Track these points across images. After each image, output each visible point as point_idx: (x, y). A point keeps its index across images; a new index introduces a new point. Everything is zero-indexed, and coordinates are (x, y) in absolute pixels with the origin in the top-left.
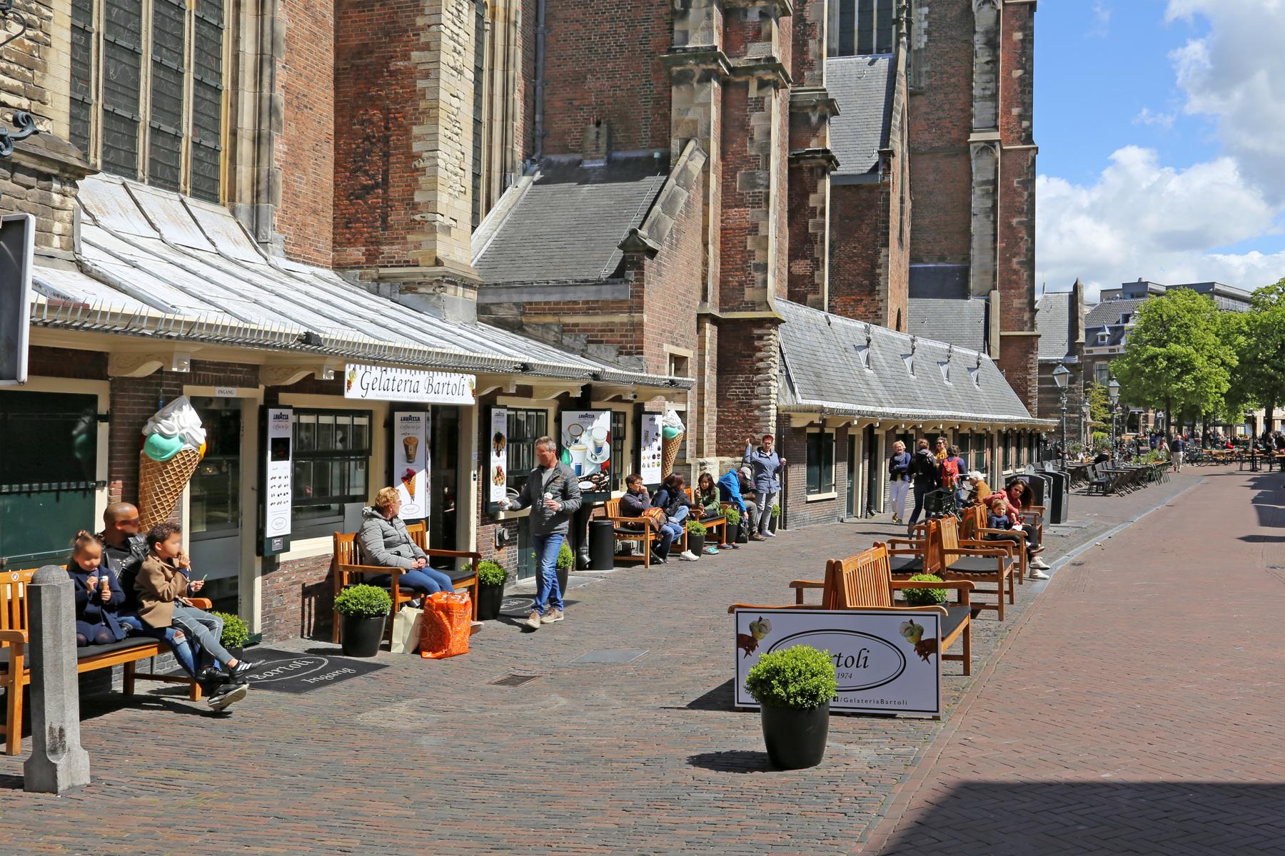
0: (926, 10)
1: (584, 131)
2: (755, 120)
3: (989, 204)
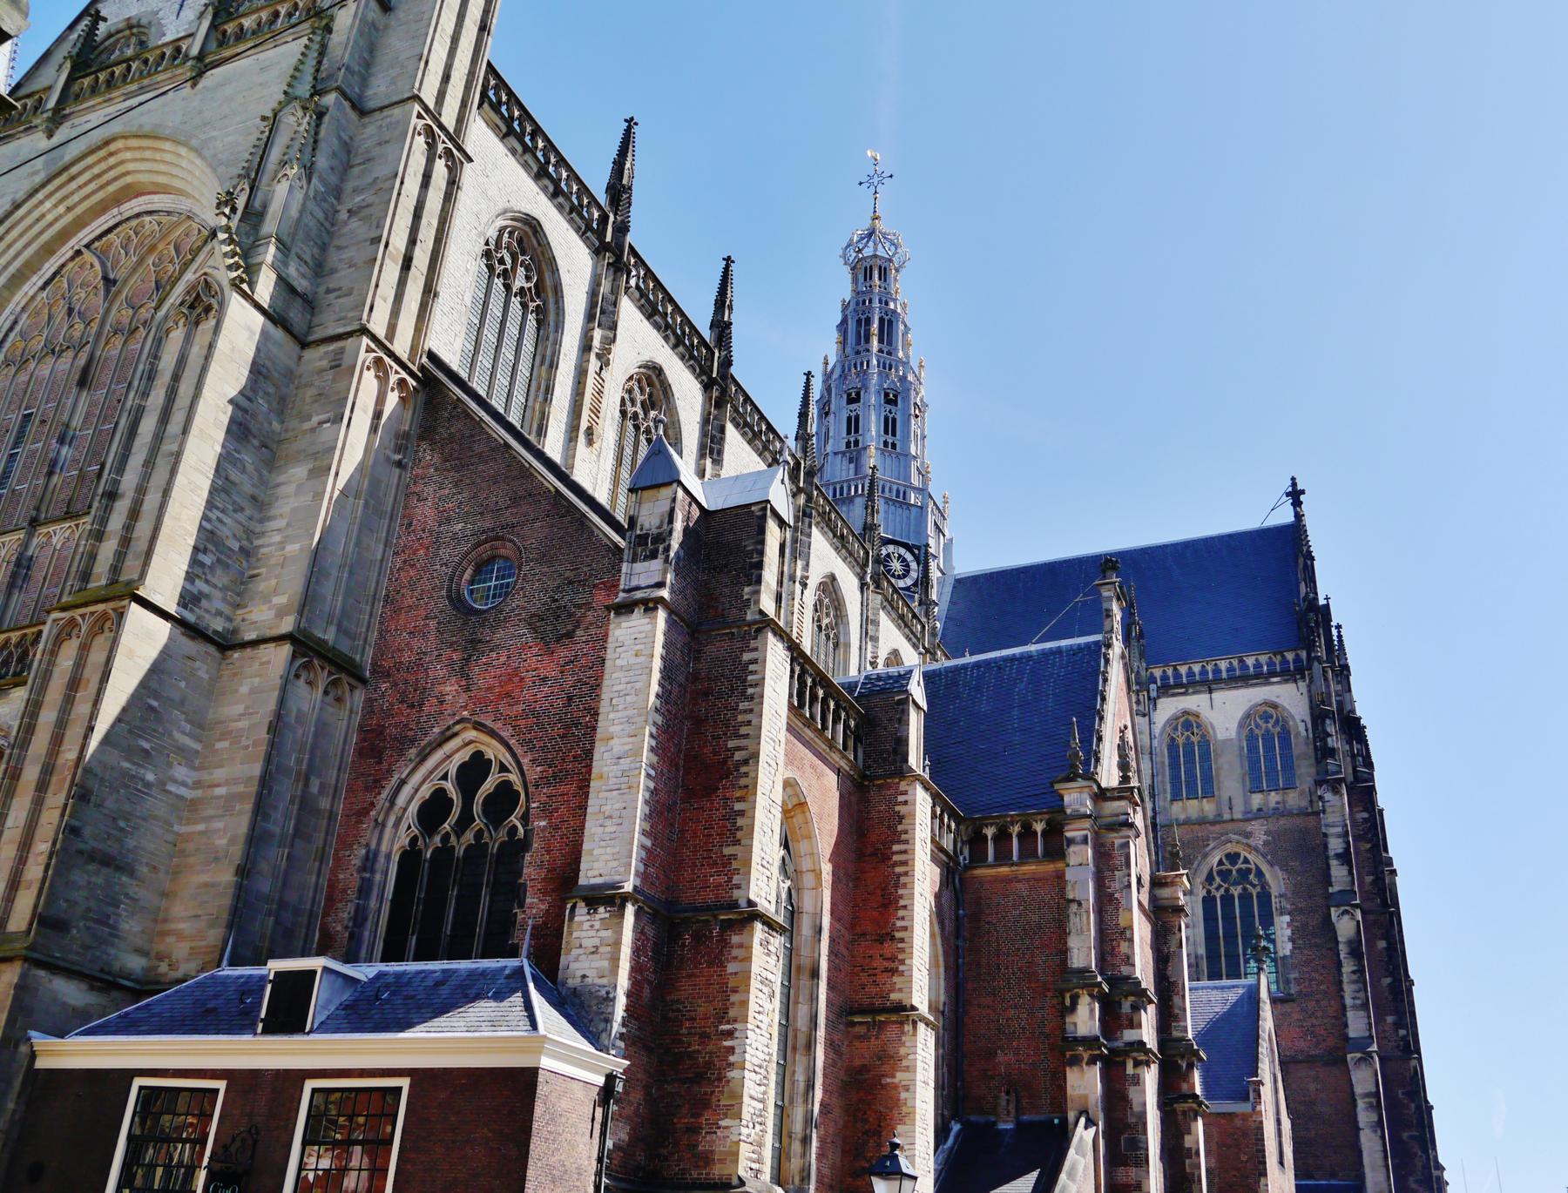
0: (1287, 918)
1: (996, 1097)
2: (1133, 1093)
3: (1375, 1118)
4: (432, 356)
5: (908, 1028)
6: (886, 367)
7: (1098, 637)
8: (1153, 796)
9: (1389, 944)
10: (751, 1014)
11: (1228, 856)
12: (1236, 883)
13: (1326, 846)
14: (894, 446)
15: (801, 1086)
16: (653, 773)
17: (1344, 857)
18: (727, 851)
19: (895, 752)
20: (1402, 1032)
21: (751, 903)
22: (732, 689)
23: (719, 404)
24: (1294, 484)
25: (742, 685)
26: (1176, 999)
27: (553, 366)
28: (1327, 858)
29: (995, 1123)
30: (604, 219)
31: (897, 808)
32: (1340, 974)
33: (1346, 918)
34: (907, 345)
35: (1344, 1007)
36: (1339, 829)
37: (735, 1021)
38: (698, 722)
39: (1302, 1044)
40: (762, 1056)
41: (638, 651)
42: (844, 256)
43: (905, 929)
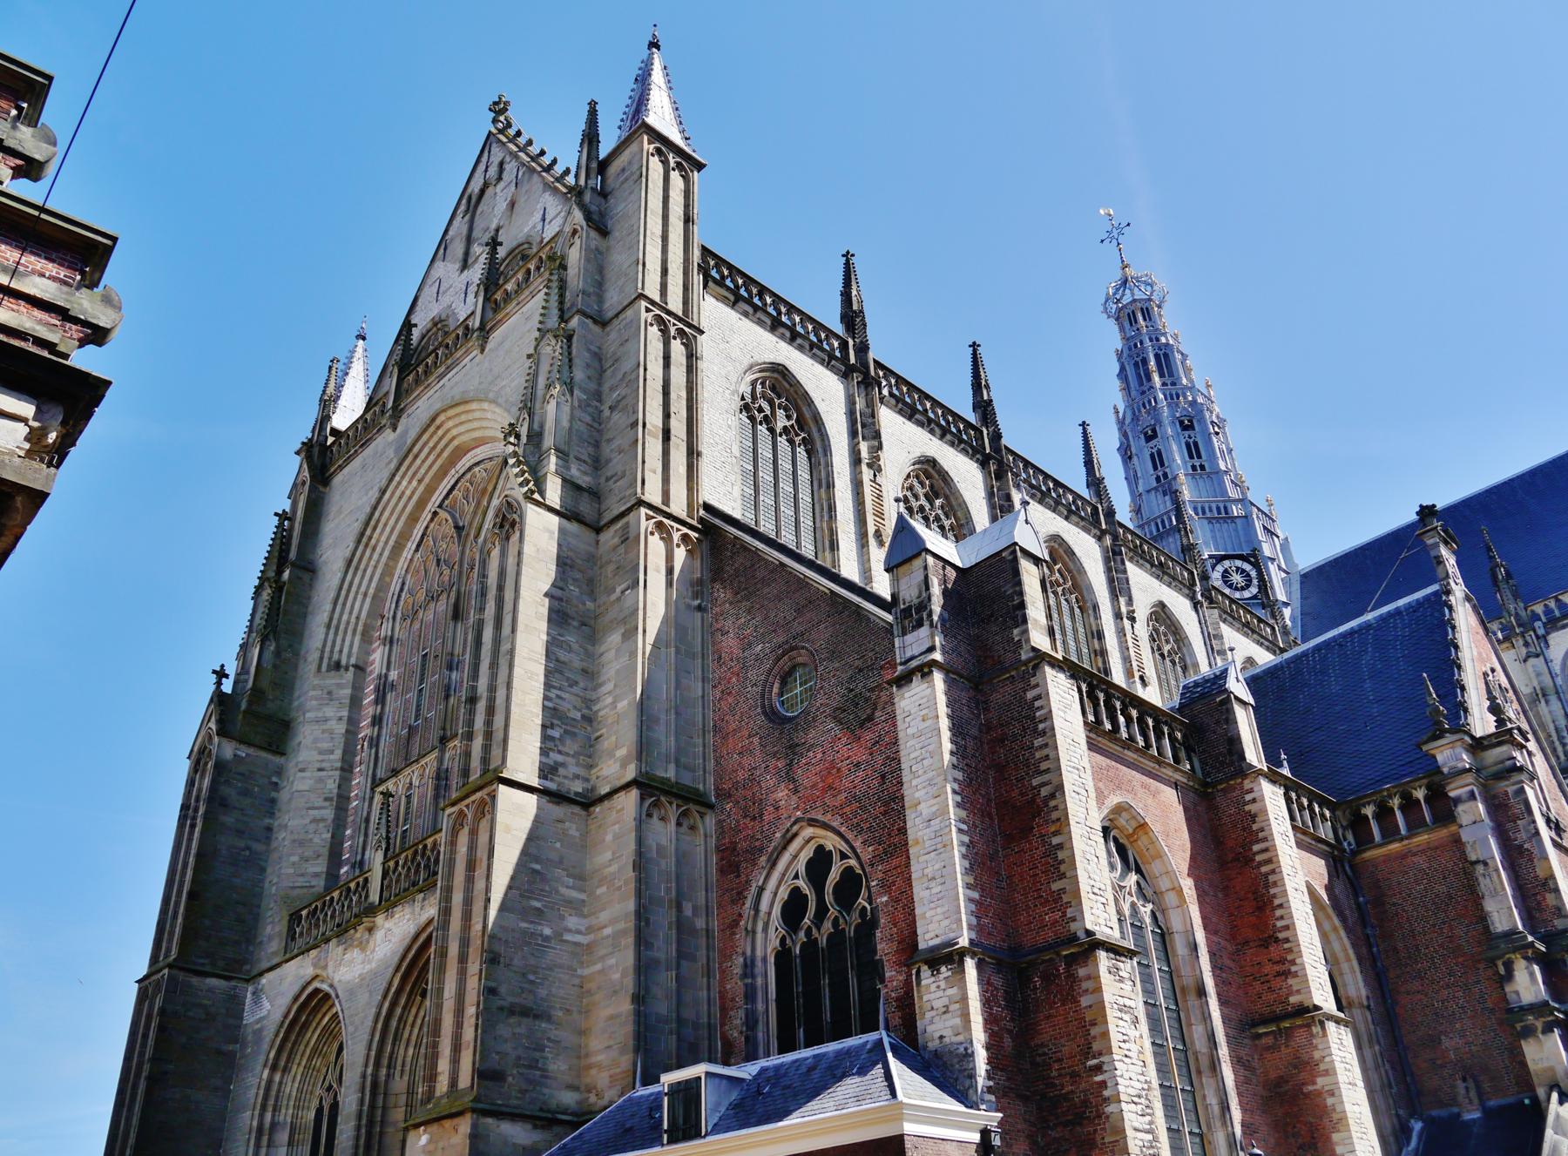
1: (1453, 1087)
4: (708, 507)
5: (1316, 1029)
6: (1173, 398)
7: (1435, 588)
10: (1114, 1044)
14: (1202, 467)
15: (1216, 1109)
16: (965, 827)
18: (1055, 886)
19: (1230, 752)
21: (1089, 933)
22: (1024, 729)
23: (1000, 475)
25: (1033, 723)
27: (830, 486)
29: (1459, 1115)
30: (844, 345)
31: (1247, 808)
34: (1188, 371)
37: (1100, 1054)
38: (1000, 768)
40: (1139, 1086)
41: (926, 714)
43: (1287, 928)
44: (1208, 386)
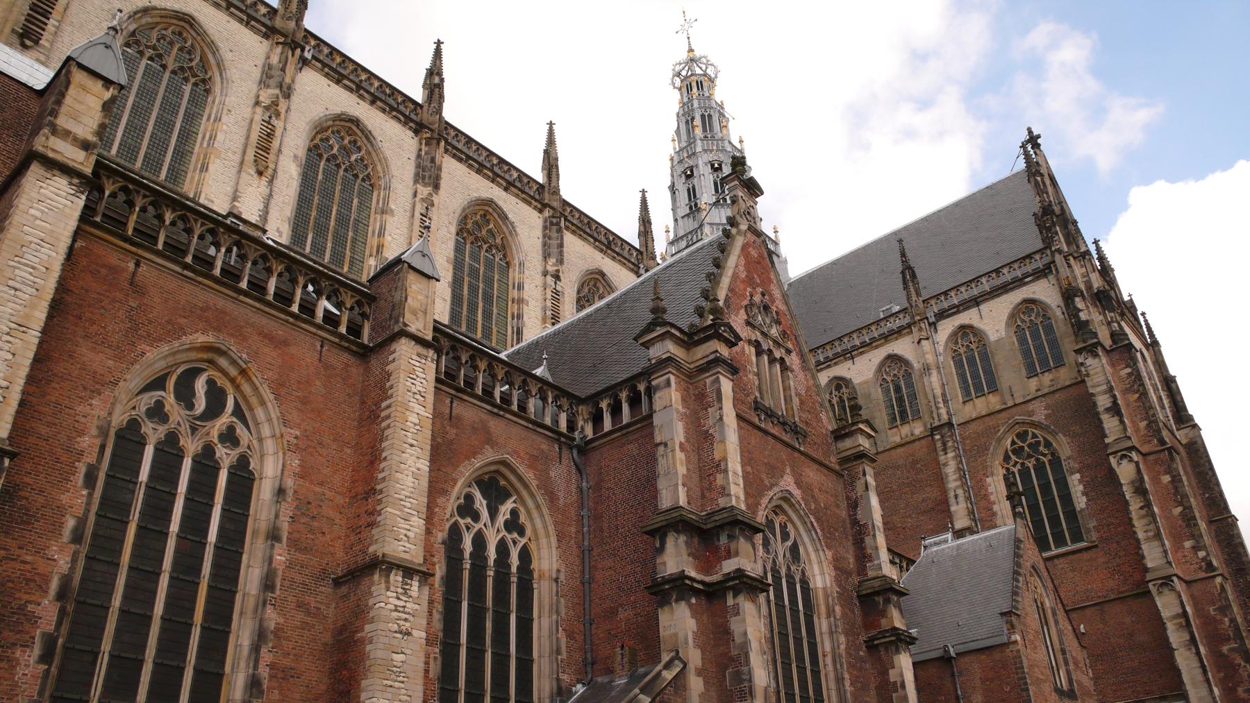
0: (1078, 476)
8: (945, 401)
9: (1173, 477)
11: (1018, 435)
12: (1030, 456)
13: (1095, 404)
17: (1115, 410)
20: (1202, 554)
24: (1030, 131)
26: (868, 540)
28: (1098, 414)
32: (1128, 512)
33: (1125, 462)
35: (1138, 541)
36: (1105, 387)
39: (1111, 584)
42: (673, 84)
44: (741, 141)
